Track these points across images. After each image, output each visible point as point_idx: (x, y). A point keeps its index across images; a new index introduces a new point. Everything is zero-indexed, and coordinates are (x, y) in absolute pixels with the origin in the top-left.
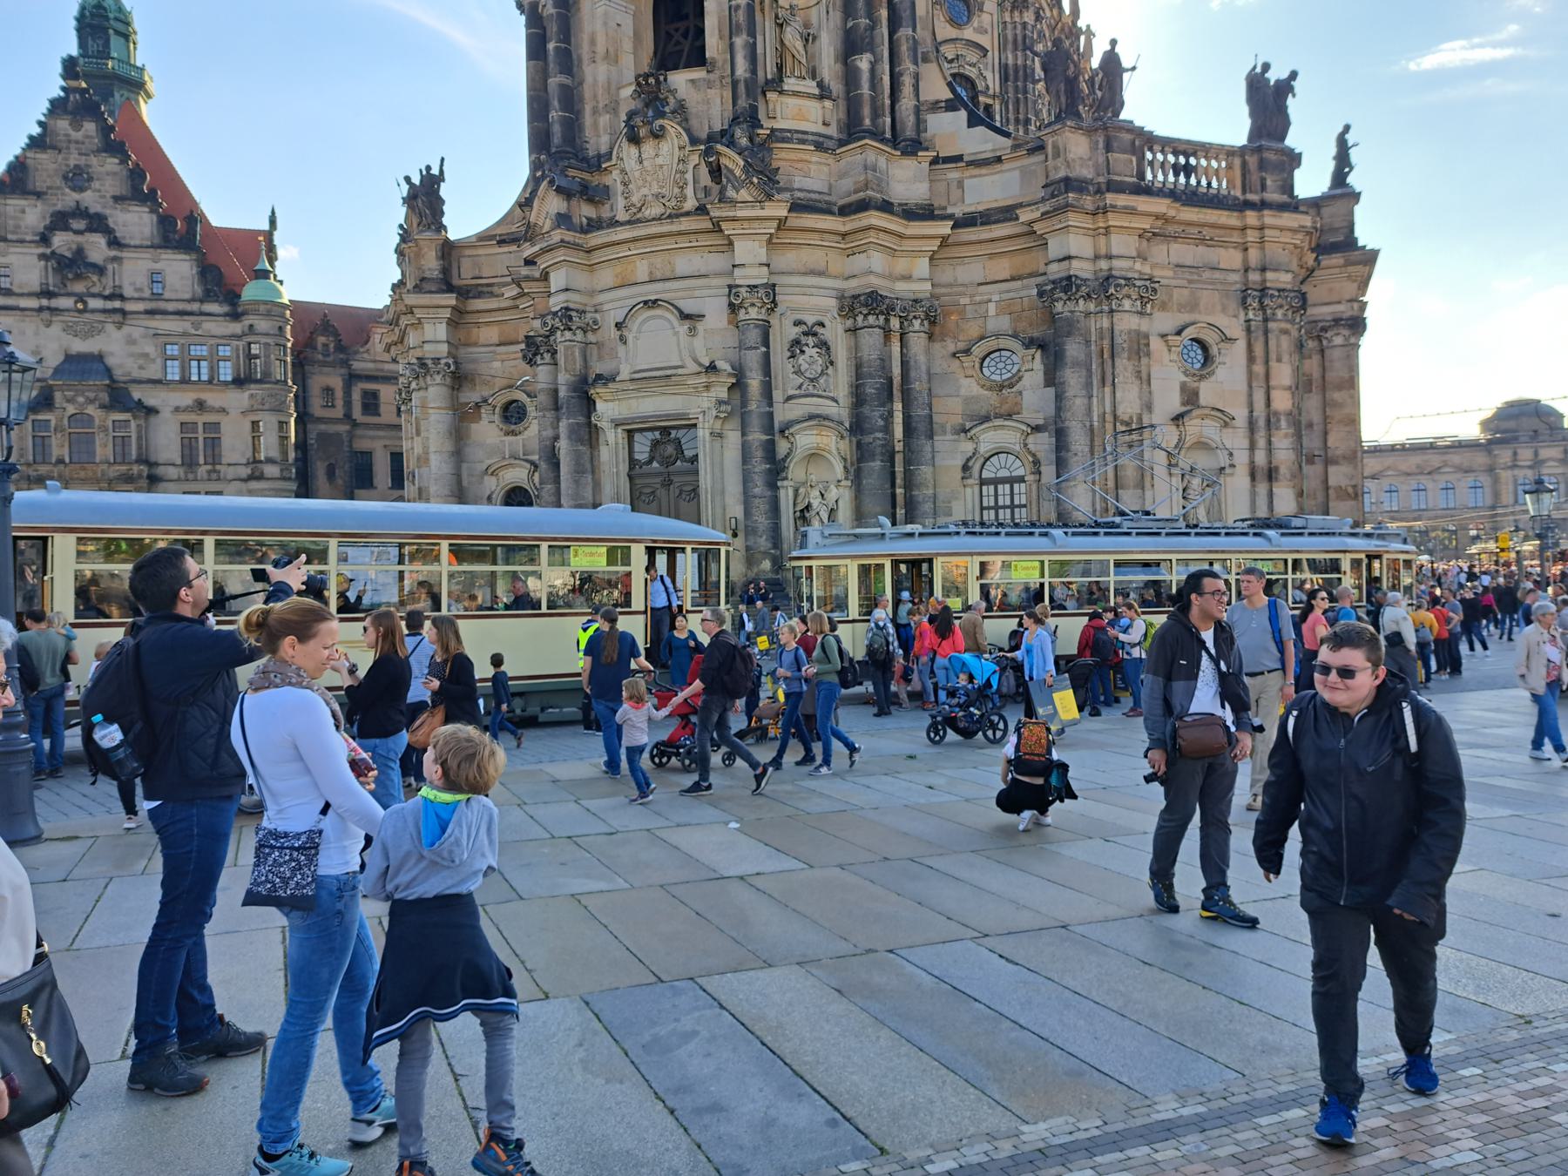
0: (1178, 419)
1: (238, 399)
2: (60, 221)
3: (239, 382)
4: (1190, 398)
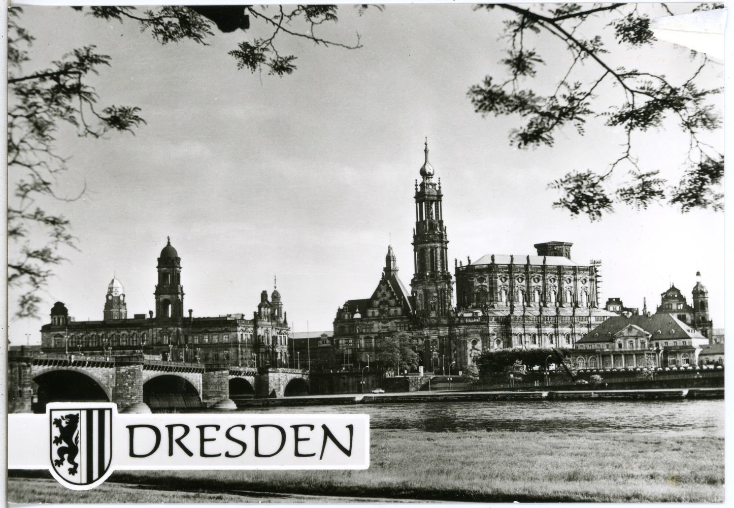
0: (471, 350)
2: (381, 303)
4: (473, 348)
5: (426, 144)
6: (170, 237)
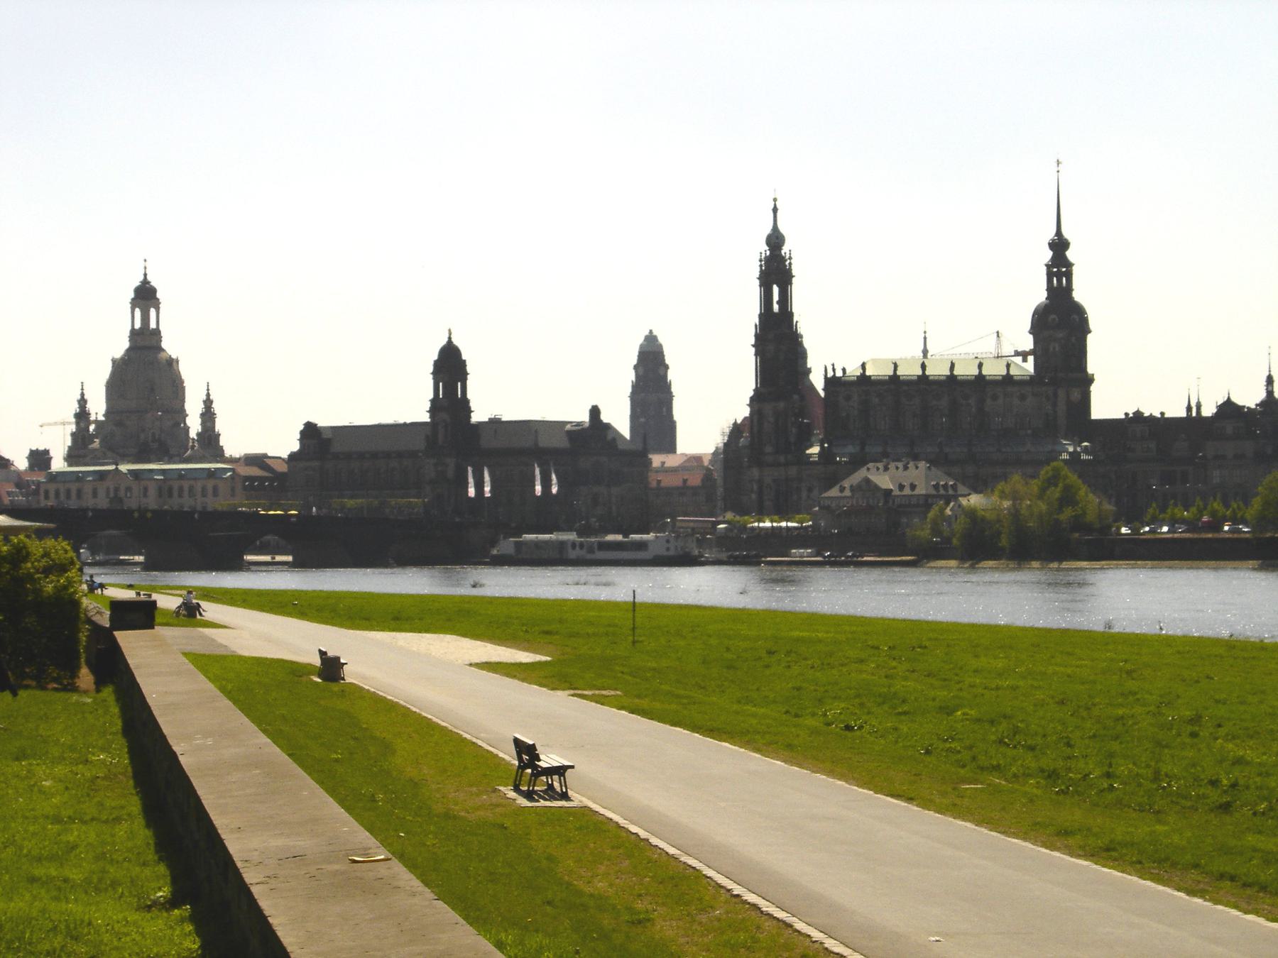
5: (775, 200)
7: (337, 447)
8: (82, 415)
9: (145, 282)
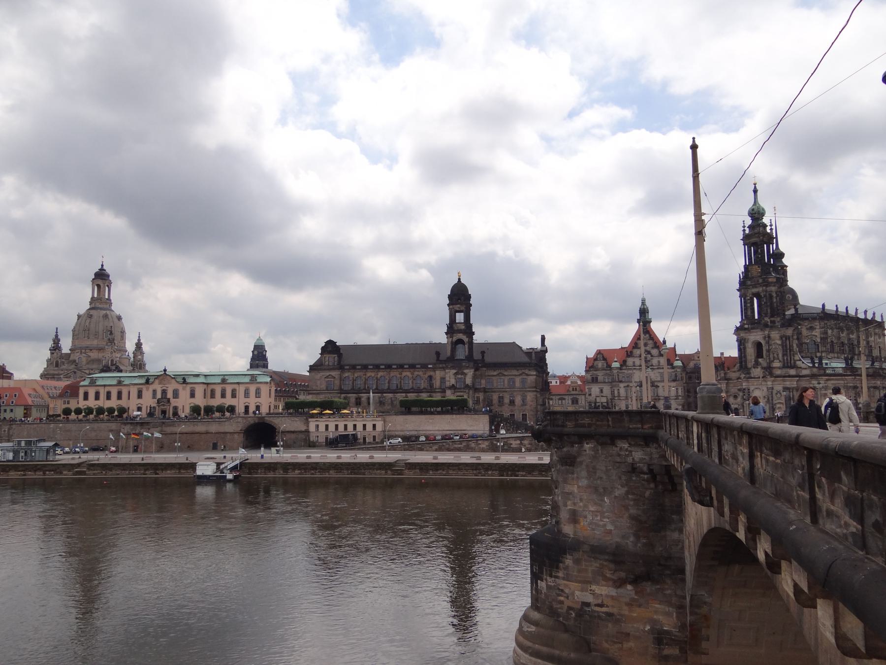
1: (674, 384)
3: (674, 381)
6: (461, 273)
7: (348, 360)
8: (56, 347)
9: (102, 269)
